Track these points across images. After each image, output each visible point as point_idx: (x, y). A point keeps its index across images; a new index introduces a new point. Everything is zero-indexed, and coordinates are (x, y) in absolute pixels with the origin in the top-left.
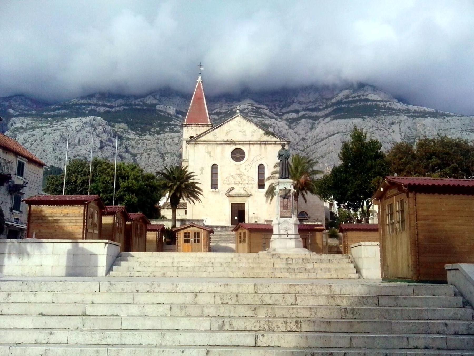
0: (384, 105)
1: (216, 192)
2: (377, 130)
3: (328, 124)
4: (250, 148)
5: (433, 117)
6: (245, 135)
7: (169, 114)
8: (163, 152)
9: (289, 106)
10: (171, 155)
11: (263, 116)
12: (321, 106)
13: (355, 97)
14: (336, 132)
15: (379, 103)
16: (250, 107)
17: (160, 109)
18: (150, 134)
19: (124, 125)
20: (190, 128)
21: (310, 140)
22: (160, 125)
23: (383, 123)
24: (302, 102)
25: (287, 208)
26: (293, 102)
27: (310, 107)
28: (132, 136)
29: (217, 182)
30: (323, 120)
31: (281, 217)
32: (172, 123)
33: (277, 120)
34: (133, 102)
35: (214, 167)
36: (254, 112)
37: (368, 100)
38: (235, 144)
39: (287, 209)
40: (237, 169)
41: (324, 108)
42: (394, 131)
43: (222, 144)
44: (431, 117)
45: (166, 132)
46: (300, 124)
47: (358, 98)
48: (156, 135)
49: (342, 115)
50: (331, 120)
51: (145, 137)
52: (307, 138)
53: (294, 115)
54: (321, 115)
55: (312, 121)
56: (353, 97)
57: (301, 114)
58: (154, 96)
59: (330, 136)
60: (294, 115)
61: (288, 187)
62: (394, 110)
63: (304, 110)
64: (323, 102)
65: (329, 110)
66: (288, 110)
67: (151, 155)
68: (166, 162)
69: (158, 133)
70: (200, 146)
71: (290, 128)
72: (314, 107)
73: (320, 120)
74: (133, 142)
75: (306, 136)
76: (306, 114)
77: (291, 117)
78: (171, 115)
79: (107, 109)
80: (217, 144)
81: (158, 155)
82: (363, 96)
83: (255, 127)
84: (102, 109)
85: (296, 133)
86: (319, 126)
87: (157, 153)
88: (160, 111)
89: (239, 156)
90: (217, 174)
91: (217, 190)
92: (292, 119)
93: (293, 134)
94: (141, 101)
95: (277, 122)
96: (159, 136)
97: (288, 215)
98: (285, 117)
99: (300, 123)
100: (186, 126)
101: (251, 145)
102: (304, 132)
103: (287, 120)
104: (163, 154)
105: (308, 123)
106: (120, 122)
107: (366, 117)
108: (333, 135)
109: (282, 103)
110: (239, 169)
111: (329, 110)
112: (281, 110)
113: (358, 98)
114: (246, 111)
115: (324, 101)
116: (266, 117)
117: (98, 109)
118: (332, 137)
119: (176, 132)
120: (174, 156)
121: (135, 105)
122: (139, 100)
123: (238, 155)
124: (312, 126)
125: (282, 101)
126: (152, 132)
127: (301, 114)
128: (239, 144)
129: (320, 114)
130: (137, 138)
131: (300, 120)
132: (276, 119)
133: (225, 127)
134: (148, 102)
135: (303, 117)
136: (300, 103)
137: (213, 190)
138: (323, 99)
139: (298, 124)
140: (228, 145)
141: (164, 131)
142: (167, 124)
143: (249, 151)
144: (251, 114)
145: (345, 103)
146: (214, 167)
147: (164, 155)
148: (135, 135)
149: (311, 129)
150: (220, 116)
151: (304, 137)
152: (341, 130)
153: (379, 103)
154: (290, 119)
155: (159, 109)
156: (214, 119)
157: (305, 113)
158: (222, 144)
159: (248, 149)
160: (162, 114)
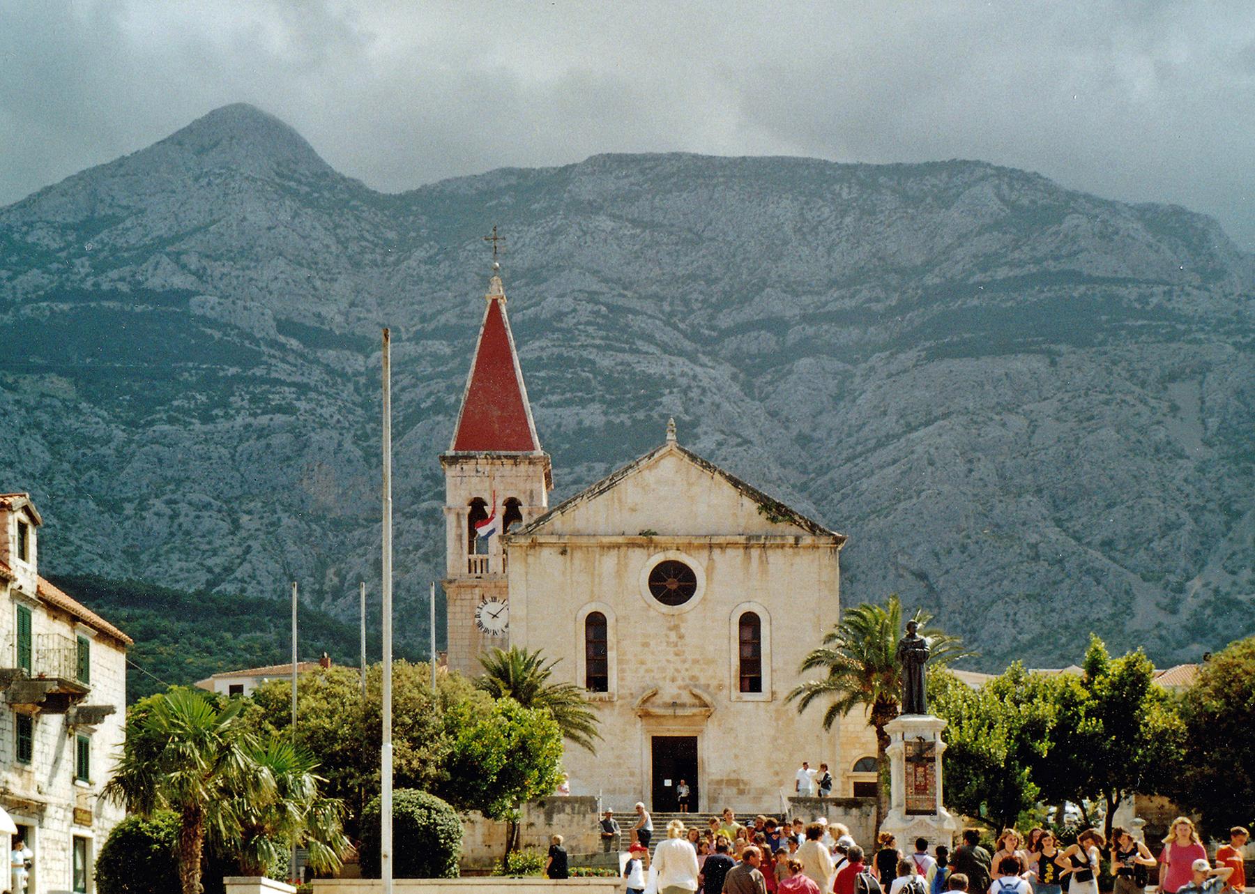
7: (243, 335)
8: (229, 494)
10: (265, 504)
11: (640, 344)
18: (171, 421)
22: (209, 381)
28: (100, 430)
32: (259, 371)
34: (88, 285)
45: (238, 412)
48: (197, 425)
51: (150, 432)
58: (177, 257)
59: (910, 428)
67: (183, 507)
68: (243, 533)
69: (207, 418)
74: (104, 450)
81: (208, 506)
87: (207, 499)
88: (204, 320)
94: (122, 279)
96: (210, 427)
104: (227, 502)
106: (41, 370)
114: (569, 322)
116: (652, 349)
118: (921, 433)
119: (279, 409)
120: (279, 508)
122: (114, 274)
126: (177, 409)
130: (119, 434)
132: (693, 358)
134: (155, 283)
141: (226, 406)
142: (236, 378)
147: (235, 505)
148: (108, 423)
150: (458, 343)
155: (199, 312)
160: (217, 335)
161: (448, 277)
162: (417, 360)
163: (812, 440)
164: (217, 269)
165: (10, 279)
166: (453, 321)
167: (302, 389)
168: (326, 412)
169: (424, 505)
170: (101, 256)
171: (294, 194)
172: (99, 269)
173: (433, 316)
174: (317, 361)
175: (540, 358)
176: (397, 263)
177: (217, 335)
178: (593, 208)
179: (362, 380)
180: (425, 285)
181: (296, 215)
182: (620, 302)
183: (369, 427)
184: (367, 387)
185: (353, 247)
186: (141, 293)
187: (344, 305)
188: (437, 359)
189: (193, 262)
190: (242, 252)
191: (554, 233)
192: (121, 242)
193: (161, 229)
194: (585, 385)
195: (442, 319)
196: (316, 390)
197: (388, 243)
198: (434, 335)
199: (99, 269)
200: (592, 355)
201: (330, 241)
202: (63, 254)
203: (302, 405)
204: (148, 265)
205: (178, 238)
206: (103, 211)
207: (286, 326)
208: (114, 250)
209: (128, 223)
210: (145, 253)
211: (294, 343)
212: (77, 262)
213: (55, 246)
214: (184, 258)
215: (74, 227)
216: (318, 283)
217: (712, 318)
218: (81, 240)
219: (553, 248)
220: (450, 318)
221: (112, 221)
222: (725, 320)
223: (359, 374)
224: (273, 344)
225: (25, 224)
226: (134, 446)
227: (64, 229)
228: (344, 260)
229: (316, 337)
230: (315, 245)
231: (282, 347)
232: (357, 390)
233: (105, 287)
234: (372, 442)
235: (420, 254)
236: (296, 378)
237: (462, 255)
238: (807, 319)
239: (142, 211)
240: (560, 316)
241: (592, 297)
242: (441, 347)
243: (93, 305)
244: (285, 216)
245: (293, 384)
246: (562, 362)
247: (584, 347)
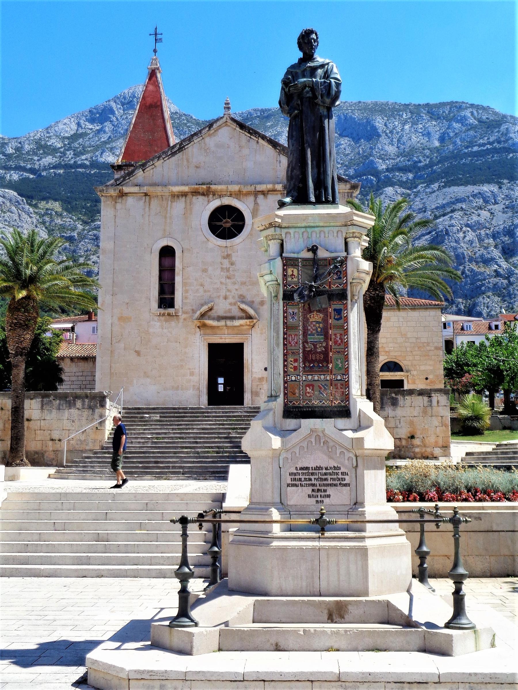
1: (169, 315)
4: (256, 203)
13: (484, 145)
19: (57, 206)
25: (326, 359)
27: (400, 165)
29: (173, 292)
31: (291, 412)
35: (167, 253)
39: (325, 370)
40: (224, 258)
46: (383, 196)
47: (489, 146)
50: (439, 188)
56: (480, 145)
61: (330, 246)
64: (424, 156)
79: (26, 174)
82: (499, 142)
84: (15, 176)
89: (228, 225)
90: (172, 270)
91: (171, 311)
94: (86, 159)
97: (329, 399)
99: (381, 194)
101: (261, 197)
107: (505, 181)
108: (444, 215)
110: (228, 256)
113: (489, 146)
115: (427, 152)
117: (8, 177)
121: (76, 166)
122: (83, 157)
123: (226, 223)
130: (80, 227)
137: (162, 311)
138: (424, 149)
140: (201, 198)
143: (255, 213)
146: (167, 253)
148: (75, 221)
158: (184, 195)
159: (252, 206)
165: (38, 160)
170: (79, 150)
172: (77, 154)
186: (94, 164)
199: (77, 154)
202: (62, 150)
212: (68, 153)
213: (59, 146)
215: (68, 138)
217: (346, 171)
225: (47, 137)
226: (86, 232)
227: (64, 138)
233: (79, 163)
243: (73, 170)
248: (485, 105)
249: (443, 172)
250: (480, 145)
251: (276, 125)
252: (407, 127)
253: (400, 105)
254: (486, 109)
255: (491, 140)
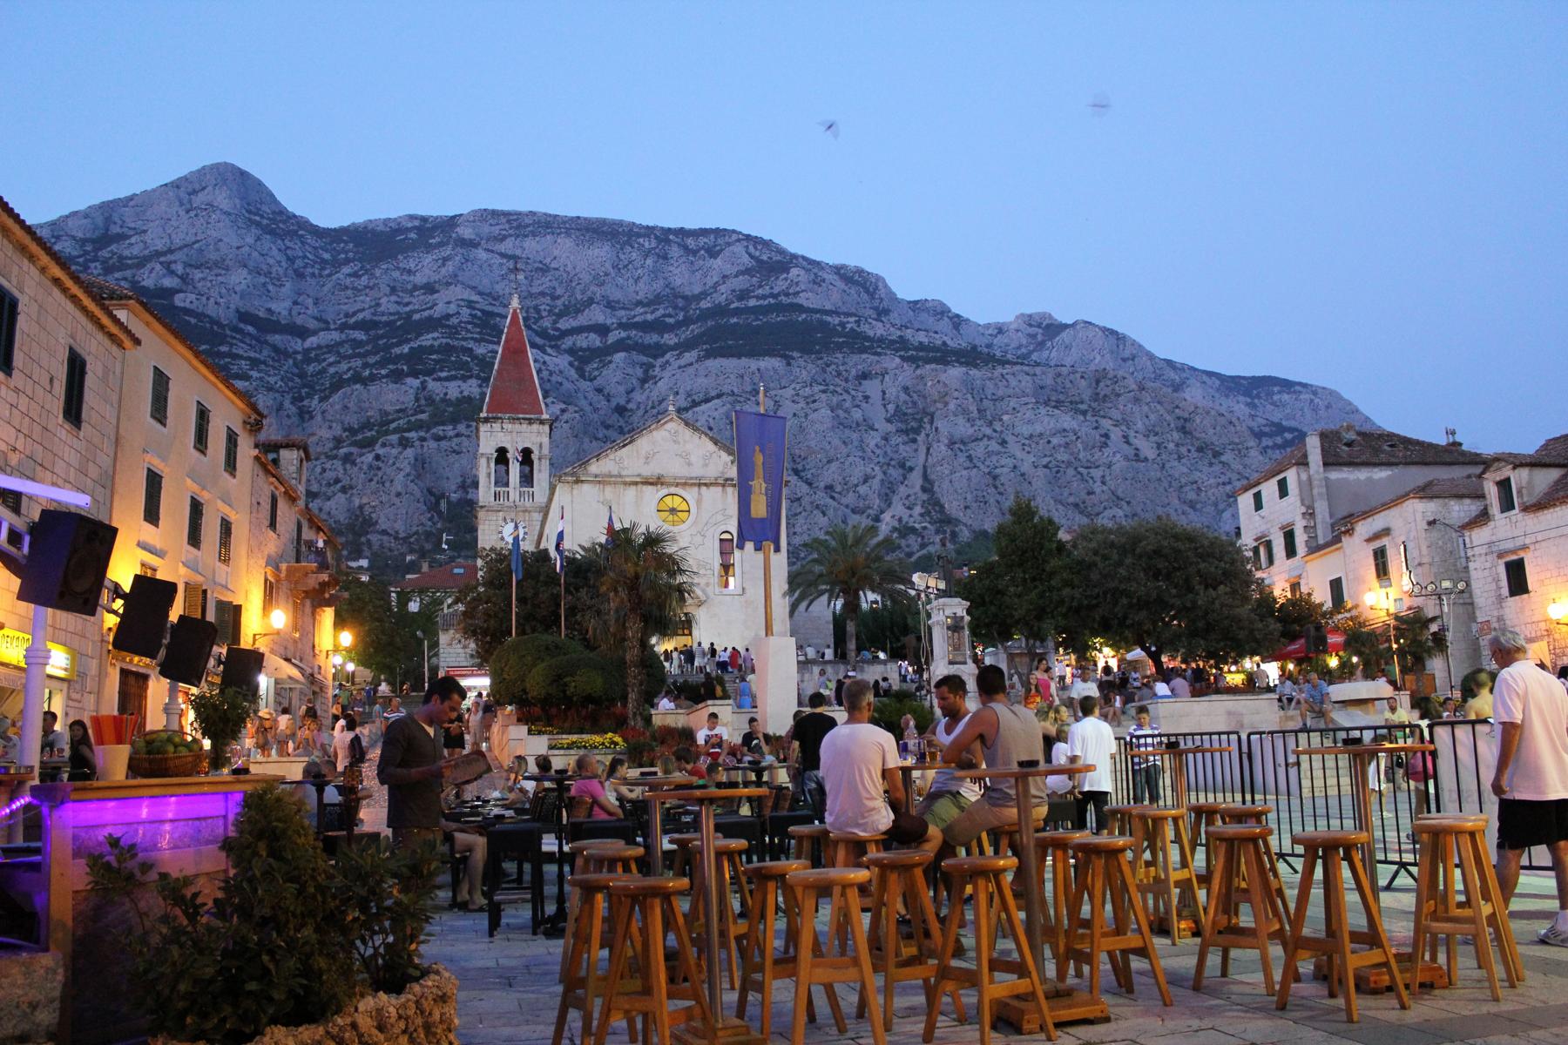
0: (843, 325)
2: (824, 392)
3: (691, 370)
5: (967, 364)
6: (689, 464)
9: (578, 311)
12: (670, 316)
13: (764, 297)
14: (713, 393)
15: (829, 319)
16: (465, 311)
17: (187, 305)
20: (497, 426)
21: (640, 413)
23: (839, 374)
24: (618, 302)
26: (591, 301)
30: (679, 357)
32: (224, 349)
33: (544, 352)
36: (476, 325)
37: (800, 308)
38: (669, 485)
41: (679, 325)
42: (867, 398)
43: (636, 483)
44: (961, 364)
46: (612, 366)
47: (772, 301)
49: (730, 347)
50: (699, 359)
52: (630, 406)
53: (594, 340)
54: (672, 343)
55: (645, 359)
56: (758, 298)
57: (612, 338)
59: (695, 404)
60: (594, 340)
62: (867, 338)
63: (621, 326)
64: (675, 307)
65: (695, 329)
66: (574, 323)
70: (586, 487)
71: (582, 376)
72: (649, 317)
73: (668, 356)
75: (628, 401)
76: (629, 338)
77: (584, 345)
78: (221, 326)
80: (625, 484)
82: (787, 295)
83: (711, 446)
85: (599, 390)
86: (667, 374)
88: (187, 311)
92: (588, 349)
93: (591, 395)
94: (125, 279)
95: (547, 358)
97: (960, 659)
98: (568, 342)
100: (486, 420)
102: (622, 389)
103: (571, 351)
105: (634, 364)
107: (795, 354)
108: (707, 401)
109: (559, 302)
111: (695, 329)
112: (555, 322)
113: (772, 301)
114: (454, 321)
115: (681, 303)
118: (704, 407)
122: (117, 275)
124: (646, 372)
125: (558, 297)
127: (612, 338)
128: (677, 485)
129: (670, 339)
131: (610, 354)
133: (644, 443)
134: (148, 282)
135: (620, 346)
136: (611, 305)
139: (606, 364)
143: (699, 502)
144: (468, 331)
145: (737, 312)
149: (644, 381)
150: (372, 333)
151: (622, 402)
152: (726, 389)
153: (829, 319)
154: (581, 349)
156: (354, 340)
157: (624, 334)
158: (636, 483)
160: (193, 321)
161: (366, 287)
162: (341, 344)
163: (626, 409)
164: (198, 275)
166: (368, 317)
167: (255, 363)
168: (272, 380)
169: (343, 451)
171: (258, 224)
173: (355, 314)
174: (266, 342)
175: (432, 346)
176: (329, 275)
177: (193, 321)
178: (473, 244)
179: (299, 357)
180: (349, 292)
181: (258, 239)
182: (490, 308)
183: (304, 391)
184: (303, 361)
185: (299, 263)
187: (288, 304)
188: (359, 344)
189: (179, 268)
190: (216, 264)
191: (445, 260)
192: (127, 253)
193: (160, 245)
194: (463, 365)
195: (360, 316)
196: (264, 363)
197: (324, 261)
198: (356, 327)
199: (108, 270)
200: (471, 345)
201: (283, 259)
203: (255, 374)
204: (146, 270)
205: (171, 251)
206: (115, 230)
207: (245, 317)
208: (121, 258)
209: (133, 240)
210: (142, 262)
211: (250, 329)
213: (75, 253)
214: (173, 266)
215: (93, 241)
216: (271, 287)
217: (555, 322)
218: (96, 250)
219: (443, 271)
220: (366, 315)
221: (121, 237)
222: (564, 324)
223: (296, 352)
224: (236, 329)
227: (84, 241)
228: (290, 271)
229: (268, 325)
230: (271, 261)
231: (241, 331)
232: (295, 364)
234: (306, 403)
235: (346, 270)
236: (252, 355)
237: (378, 272)
238: (621, 326)
239: (145, 232)
240: (448, 316)
241: (470, 304)
242: (359, 335)
244: (250, 240)
245: (249, 358)
246: (448, 349)
247: (465, 339)
248: (766, 237)
249: (703, 334)
250: (758, 298)
251: (447, 244)
252: (649, 262)
253: (641, 227)
254: (767, 244)
255: (776, 291)
